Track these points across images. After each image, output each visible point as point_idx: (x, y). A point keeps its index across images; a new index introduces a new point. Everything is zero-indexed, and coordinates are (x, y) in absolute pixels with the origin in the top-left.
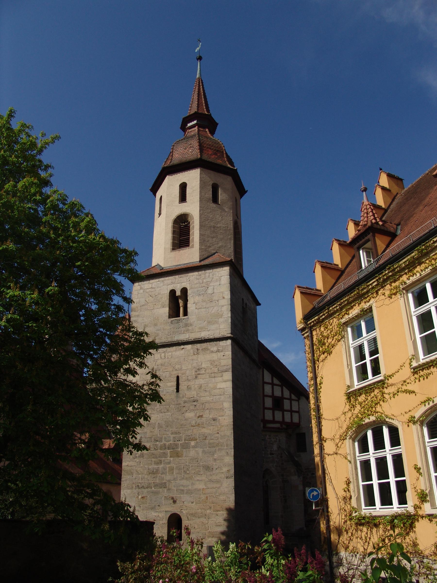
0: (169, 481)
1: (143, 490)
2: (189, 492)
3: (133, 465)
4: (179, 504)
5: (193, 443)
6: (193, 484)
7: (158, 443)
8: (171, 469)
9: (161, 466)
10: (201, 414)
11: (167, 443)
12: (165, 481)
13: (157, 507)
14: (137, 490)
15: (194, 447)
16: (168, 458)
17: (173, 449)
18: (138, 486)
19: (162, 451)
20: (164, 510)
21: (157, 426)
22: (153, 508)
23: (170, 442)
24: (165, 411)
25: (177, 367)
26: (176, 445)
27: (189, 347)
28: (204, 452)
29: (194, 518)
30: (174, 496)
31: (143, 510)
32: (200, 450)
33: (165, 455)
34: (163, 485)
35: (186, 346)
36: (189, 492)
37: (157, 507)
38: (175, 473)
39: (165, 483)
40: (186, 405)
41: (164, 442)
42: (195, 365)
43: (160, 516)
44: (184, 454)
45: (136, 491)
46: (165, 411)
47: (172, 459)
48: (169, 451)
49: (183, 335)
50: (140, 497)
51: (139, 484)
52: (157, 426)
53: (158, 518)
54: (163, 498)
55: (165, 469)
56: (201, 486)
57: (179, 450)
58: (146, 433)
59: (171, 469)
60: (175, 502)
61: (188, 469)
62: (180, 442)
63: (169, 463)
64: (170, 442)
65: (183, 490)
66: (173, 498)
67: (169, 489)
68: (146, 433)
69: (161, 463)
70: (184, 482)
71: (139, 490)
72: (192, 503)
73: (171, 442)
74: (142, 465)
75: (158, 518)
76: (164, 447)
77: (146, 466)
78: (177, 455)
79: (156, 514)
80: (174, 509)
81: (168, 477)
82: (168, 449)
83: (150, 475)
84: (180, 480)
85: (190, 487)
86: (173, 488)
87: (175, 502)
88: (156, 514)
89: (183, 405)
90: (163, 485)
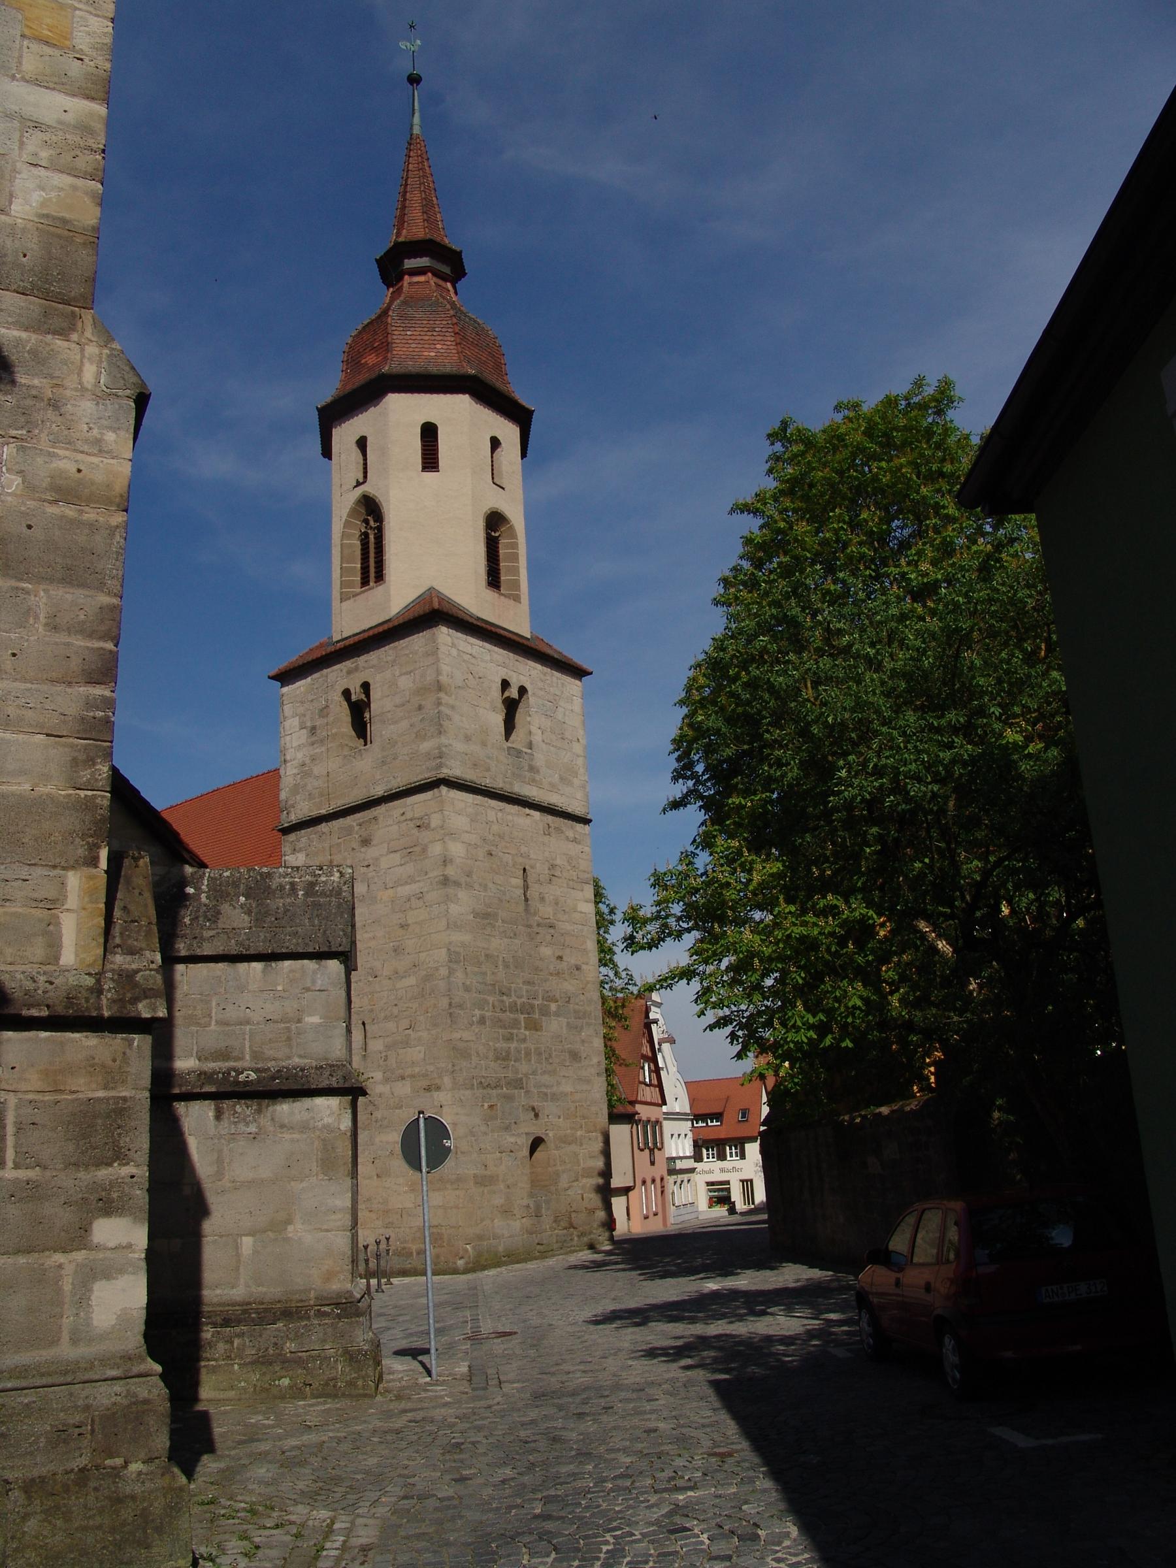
0: (526, 1075)
1: (490, 1091)
2: (554, 1097)
3: (470, 1038)
4: (543, 1120)
5: (553, 1007)
6: (559, 1083)
7: (505, 997)
8: (528, 1054)
9: (513, 1045)
10: (560, 954)
11: (519, 1002)
12: (520, 1076)
13: (513, 1126)
14: (481, 1091)
15: (557, 1014)
16: (522, 1031)
17: (528, 1014)
18: (481, 1083)
19: (512, 1016)
20: (522, 1130)
21: (500, 963)
22: (507, 1128)
23: (523, 1000)
24: (512, 935)
25: (523, 849)
26: (532, 1006)
27: (536, 814)
28: (568, 1023)
29: (563, 1145)
30: (535, 1104)
31: (493, 1131)
32: (563, 1021)
33: (515, 1024)
34: (518, 1084)
35: (532, 812)
36: (554, 1097)
37: (513, 1126)
38: (533, 1062)
39: (521, 1079)
40: (540, 930)
41: (514, 998)
42: (547, 854)
43: (519, 1143)
44: (544, 1024)
45: (479, 1092)
46: (512, 935)
47: (527, 1033)
48: (523, 1016)
49: (529, 786)
50: (486, 1105)
51: (483, 1080)
52: (500, 963)
53: (517, 1147)
54: (520, 1110)
55: (519, 1052)
56: (567, 1088)
57: (537, 1016)
58: (485, 974)
59: (528, 1054)
60: (536, 1116)
61: (550, 1056)
62: (536, 1002)
63: (524, 1040)
64: (523, 1000)
65: (546, 1094)
66: (533, 1109)
67: (527, 1092)
68: (485, 974)
69: (513, 1039)
70: (546, 1079)
71: (485, 1091)
72: (559, 1117)
73: (524, 1000)
74: (483, 1041)
75: (517, 1147)
76: (513, 1008)
77: (491, 1043)
78: (534, 1026)
79: (512, 1140)
80: (536, 1130)
81: (524, 1067)
82: (522, 1013)
83: (499, 1062)
84: (541, 1074)
85: (555, 1089)
86: (532, 1089)
87: (536, 1116)
88: (512, 1140)
89: (536, 929)
90: (518, 1084)
